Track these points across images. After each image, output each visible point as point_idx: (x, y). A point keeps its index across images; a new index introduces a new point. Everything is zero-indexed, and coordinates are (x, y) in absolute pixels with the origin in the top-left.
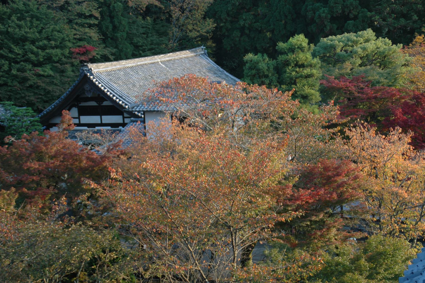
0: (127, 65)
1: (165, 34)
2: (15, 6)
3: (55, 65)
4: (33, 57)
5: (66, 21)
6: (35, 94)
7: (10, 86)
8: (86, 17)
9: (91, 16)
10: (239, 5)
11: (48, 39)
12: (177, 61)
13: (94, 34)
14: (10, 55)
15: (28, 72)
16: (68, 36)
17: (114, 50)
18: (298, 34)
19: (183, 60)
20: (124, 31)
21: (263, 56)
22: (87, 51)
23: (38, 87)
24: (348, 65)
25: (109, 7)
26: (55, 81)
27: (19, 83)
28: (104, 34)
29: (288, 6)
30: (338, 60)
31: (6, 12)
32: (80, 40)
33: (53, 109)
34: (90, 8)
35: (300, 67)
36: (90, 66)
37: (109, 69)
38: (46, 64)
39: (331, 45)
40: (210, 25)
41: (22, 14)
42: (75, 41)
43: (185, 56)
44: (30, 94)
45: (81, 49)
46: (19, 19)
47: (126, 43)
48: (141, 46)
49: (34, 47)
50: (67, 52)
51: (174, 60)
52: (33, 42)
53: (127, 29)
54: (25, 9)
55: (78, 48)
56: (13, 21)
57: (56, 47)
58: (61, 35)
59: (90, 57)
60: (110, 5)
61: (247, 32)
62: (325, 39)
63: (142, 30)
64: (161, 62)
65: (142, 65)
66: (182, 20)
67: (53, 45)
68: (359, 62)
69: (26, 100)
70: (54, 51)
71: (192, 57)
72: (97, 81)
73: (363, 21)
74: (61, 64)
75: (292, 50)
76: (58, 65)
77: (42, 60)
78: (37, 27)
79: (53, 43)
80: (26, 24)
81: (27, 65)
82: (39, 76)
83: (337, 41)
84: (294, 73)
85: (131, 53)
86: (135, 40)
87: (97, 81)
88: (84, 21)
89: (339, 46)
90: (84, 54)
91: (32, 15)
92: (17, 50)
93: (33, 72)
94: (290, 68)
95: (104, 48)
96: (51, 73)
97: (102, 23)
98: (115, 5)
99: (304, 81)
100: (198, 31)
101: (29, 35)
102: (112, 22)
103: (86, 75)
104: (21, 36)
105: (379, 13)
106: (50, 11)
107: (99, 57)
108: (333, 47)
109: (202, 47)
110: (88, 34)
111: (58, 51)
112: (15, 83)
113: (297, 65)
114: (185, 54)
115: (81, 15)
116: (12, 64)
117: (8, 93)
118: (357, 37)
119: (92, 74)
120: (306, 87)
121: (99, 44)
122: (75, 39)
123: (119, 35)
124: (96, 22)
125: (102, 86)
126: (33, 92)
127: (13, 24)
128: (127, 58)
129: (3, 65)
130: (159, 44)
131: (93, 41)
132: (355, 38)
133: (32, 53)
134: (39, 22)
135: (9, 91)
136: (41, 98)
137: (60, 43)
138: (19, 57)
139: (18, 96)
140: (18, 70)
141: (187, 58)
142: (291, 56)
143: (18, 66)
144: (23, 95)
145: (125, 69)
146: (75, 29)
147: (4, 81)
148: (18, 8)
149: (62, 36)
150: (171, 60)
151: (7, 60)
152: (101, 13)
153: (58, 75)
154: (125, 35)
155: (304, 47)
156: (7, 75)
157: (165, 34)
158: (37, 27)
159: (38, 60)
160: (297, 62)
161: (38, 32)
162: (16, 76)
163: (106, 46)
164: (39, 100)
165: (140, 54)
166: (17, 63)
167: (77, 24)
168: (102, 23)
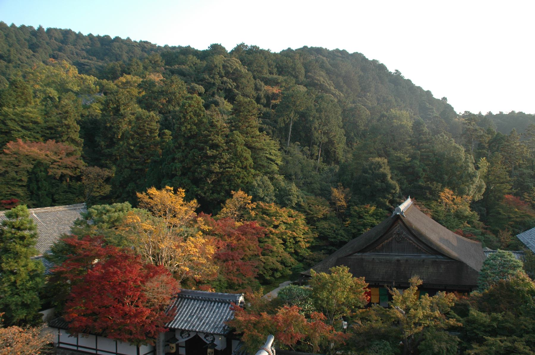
9: (21, 180)
28: (32, 192)
32: (11, 195)
45: (9, 201)
64: (35, 213)
71: (65, 210)
73: (192, 193)
102: (37, 184)
105: (202, 189)
115: (13, 179)
124: (25, 184)
152: (29, 178)
163: (31, 200)
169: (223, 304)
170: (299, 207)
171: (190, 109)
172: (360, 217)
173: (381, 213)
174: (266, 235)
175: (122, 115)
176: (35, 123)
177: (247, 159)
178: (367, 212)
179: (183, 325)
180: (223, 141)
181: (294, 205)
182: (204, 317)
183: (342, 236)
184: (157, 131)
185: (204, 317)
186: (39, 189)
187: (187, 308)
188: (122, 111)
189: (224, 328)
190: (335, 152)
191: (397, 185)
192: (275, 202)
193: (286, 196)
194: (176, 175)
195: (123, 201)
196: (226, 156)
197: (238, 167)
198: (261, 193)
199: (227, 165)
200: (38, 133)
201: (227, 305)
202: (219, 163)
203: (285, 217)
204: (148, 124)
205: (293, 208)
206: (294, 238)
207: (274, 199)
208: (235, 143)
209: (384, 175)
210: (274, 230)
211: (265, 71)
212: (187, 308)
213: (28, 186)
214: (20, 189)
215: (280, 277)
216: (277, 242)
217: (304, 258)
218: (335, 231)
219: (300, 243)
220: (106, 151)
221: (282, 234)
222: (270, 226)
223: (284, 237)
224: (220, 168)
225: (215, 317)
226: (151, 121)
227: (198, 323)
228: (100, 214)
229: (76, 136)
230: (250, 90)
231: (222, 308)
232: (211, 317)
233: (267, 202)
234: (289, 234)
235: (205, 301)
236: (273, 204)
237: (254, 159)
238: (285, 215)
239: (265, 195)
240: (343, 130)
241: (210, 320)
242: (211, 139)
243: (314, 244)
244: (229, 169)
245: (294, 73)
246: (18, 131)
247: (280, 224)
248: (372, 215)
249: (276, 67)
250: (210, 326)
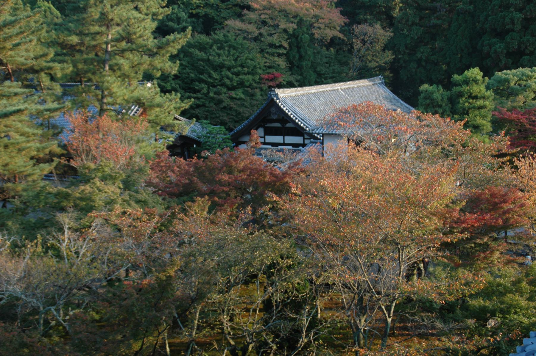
0: (310, 92)
1: (346, 64)
2: (216, 37)
3: (247, 89)
4: (228, 82)
5: (259, 50)
6: (228, 114)
7: (208, 107)
8: (276, 47)
9: (281, 46)
10: (418, 38)
11: (242, 66)
12: (356, 89)
13: (282, 62)
14: (209, 80)
15: (223, 95)
16: (259, 64)
17: (299, 77)
18: (474, 67)
19: (361, 89)
20: (309, 60)
21: (438, 87)
22: (275, 77)
23: (231, 109)
24: (520, 99)
25: (297, 38)
26: (245, 103)
27: (215, 104)
28: (291, 63)
29: (464, 41)
30: (512, 93)
31: (208, 42)
32: (270, 67)
33: (242, 129)
34: (281, 39)
35: (473, 98)
36: (277, 91)
37: (294, 94)
38: (239, 88)
39: (505, 78)
40: (389, 56)
41: (221, 44)
42: (265, 69)
43: (364, 84)
44: (223, 115)
45: (270, 75)
46: (219, 48)
47: (310, 71)
48: (324, 74)
49: (229, 73)
50: (257, 78)
51: (354, 88)
52: (229, 69)
53: (312, 58)
54: (224, 40)
55: (267, 75)
56: (214, 50)
57: (249, 73)
58: (253, 63)
59: (277, 83)
60: (298, 36)
61: (424, 64)
62: (500, 73)
63: (325, 60)
64: (341, 90)
65: (323, 92)
66: (363, 51)
67: (246, 72)
68: (533, 95)
69: (220, 120)
70: (246, 77)
71: (370, 86)
72: (282, 104)
74: (252, 89)
75: (466, 82)
76: (249, 89)
77: (235, 84)
78: (233, 55)
79: (246, 70)
80: (224, 53)
81: (223, 89)
82: (232, 98)
83: (511, 75)
84: (467, 104)
85: (314, 80)
86: (318, 69)
87: (282, 104)
88: (274, 50)
89: (513, 80)
90: (272, 80)
91: (230, 45)
92: (215, 75)
93: (228, 95)
94: (464, 99)
95: (290, 75)
96: (243, 96)
97: (290, 52)
98: (303, 37)
99: (477, 112)
100: (377, 62)
101: (226, 63)
102: (299, 52)
103: (273, 99)
104: (220, 63)
106: (245, 41)
107: (285, 83)
108: (507, 81)
109: (380, 77)
110: (277, 63)
111: (250, 77)
112: (212, 104)
113: (471, 96)
115: (271, 45)
116: (211, 88)
117: (206, 113)
118: (532, 72)
119: (278, 99)
120: (478, 118)
121: (286, 72)
122: (265, 66)
123: (304, 64)
124: (285, 52)
125: (287, 109)
126: (227, 113)
127: (213, 53)
128: (310, 85)
129: (203, 88)
130: (340, 73)
131: (281, 69)
132: (530, 73)
133: (228, 78)
134: (235, 51)
135: (206, 112)
136: (232, 118)
137: (252, 70)
138: (216, 81)
139: (213, 116)
140: (215, 93)
141: (366, 86)
142: (465, 88)
143: (215, 89)
144: (218, 115)
145: (308, 94)
146: (266, 58)
147: (203, 102)
148: (218, 39)
149: (254, 64)
150: (351, 88)
151: (206, 84)
152: (290, 44)
153: (248, 98)
154: (309, 64)
155: (479, 80)
156: (205, 97)
157: (346, 64)
158: (233, 55)
159: (232, 85)
160: (471, 94)
161: (234, 60)
162: (213, 98)
164: (231, 120)
165: (323, 81)
166: (214, 86)
167: (267, 53)
168: (290, 52)
194: (513, 30)
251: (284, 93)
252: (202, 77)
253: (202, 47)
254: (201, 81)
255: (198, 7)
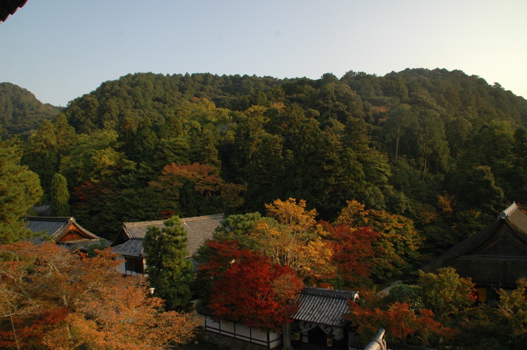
4: (139, 216)
9: (174, 196)
11: (151, 206)
28: (183, 205)
50: (158, 214)
57: (152, 211)
71: (208, 220)
79: (151, 209)
111: (153, 213)
114: (202, 218)
115: (169, 195)
119: (126, 228)
124: (177, 199)
152: (181, 194)
169: (340, 300)
170: (407, 213)
171: (308, 131)
172: (466, 222)
173: (486, 218)
174: (378, 239)
175: (251, 139)
176: (184, 149)
177: (359, 172)
178: (473, 217)
179: (306, 317)
180: (337, 157)
181: (403, 211)
182: (323, 311)
183: (449, 239)
184: (281, 151)
185: (323, 311)
186: (188, 202)
187: (309, 302)
188: (251, 136)
189: (341, 320)
190: (440, 162)
191: (501, 191)
192: (385, 209)
193: (396, 203)
195: (253, 212)
196: (341, 170)
197: (352, 179)
198: (373, 201)
199: (342, 178)
200: (186, 157)
201: (344, 301)
202: (335, 177)
203: (395, 223)
204: (273, 146)
205: (402, 214)
206: (404, 241)
207: (385, 206)
208: (348, 158)
209: (488, 182)
210: (385, 235)
211: (372, 93)
212: (309, 302)
213: (180, 200)
214: (174, 203)
215: (392, 277)
216: (388, 246)
217: (414, 260)
218: (442, 235)
219: (409, 246)
220: (239, 169)
221: (393, 238)
222: (381, 231)
223: (395, 241)
224: (336, 180)
225: (334, 311)
226: (275, 143)
227: (319, 315)
228: (236, 222)
229: (215, 159)
230: (359, 111)
231: (339, 303)
232: (330, 311)
233: (379, 210)
234: (399, 238)
235: (324, 297)
236: (384, 212)
237: (366, 172)
238: (395, 221)
239: (376, 204)
240: (446, 142)
241: (329, 313)
242: (326, 156)
243: (422, 247)
244: (343, 182)
245: (398, 94)
246: (172, 157)
247: (391, 229)
248: (476, 220)
249: (382, 89)
250: (329, 319)
251: (132, 225)
252: (127, 213)
253: (131, 196)
254: (126, 215)
255: (143, 174)
